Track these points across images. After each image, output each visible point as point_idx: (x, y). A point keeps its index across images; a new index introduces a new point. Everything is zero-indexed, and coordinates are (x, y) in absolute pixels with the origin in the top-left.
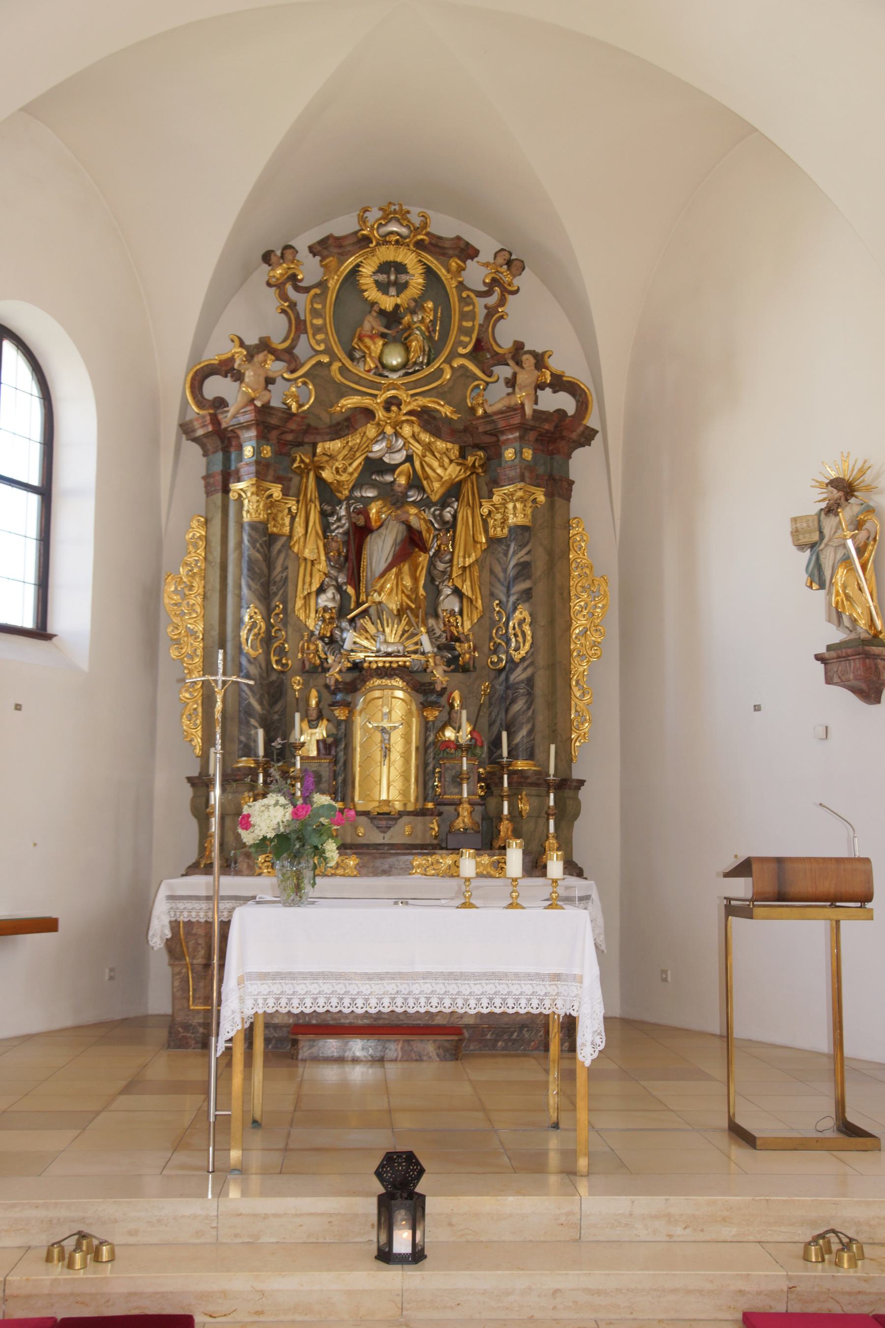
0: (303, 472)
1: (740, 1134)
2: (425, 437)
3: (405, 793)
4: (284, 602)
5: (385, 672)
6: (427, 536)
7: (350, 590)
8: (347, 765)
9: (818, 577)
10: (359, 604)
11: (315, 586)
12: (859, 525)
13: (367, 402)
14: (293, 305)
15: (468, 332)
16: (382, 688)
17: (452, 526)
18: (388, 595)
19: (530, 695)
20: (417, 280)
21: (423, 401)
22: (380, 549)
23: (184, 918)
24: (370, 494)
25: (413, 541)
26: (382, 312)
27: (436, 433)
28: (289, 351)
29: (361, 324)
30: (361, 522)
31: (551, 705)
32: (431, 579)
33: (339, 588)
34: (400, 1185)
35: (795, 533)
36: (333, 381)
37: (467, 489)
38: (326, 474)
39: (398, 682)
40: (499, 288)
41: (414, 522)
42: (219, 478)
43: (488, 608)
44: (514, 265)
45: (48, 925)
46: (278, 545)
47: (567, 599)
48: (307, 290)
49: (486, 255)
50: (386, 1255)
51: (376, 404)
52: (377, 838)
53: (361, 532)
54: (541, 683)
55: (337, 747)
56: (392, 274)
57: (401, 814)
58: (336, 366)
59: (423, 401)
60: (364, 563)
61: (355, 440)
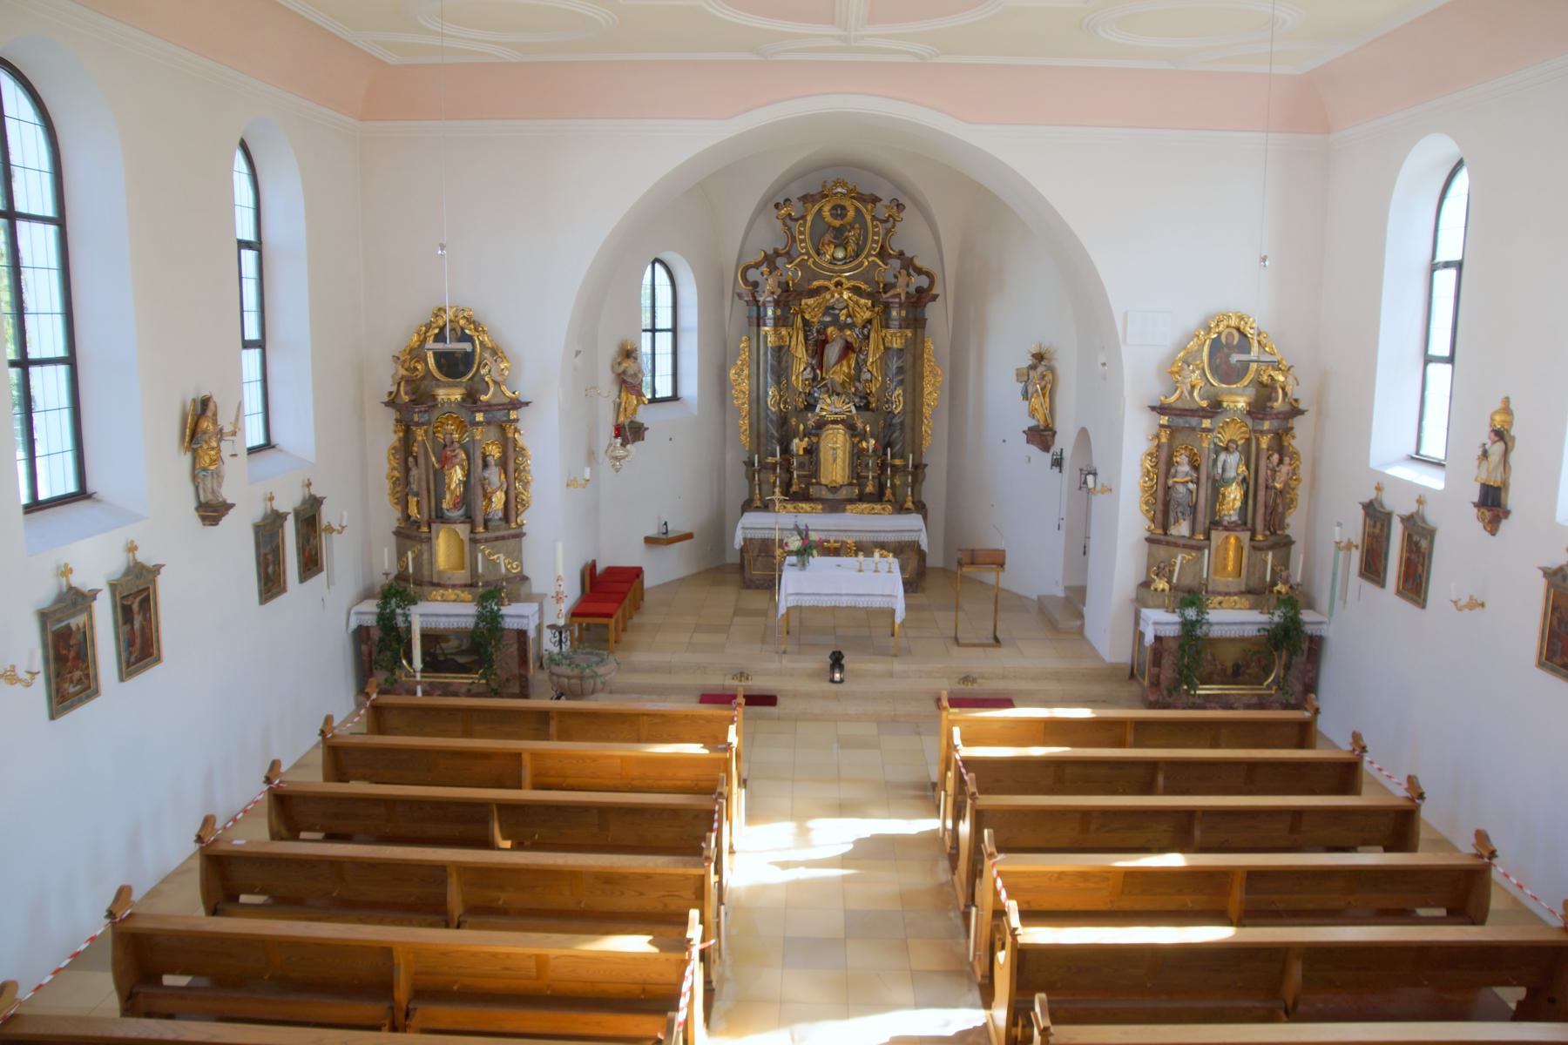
0: (795, 314)
1: (956, 641)
2: (855, 298)
5: (835, 422)
6: (856, 346)
8: (818, 463)
9: (1026, 395)
12: (1043, 377)
15: (877, 242)
17: (868, 337)
18: (838, 373)
19: (902, 430)
20: (851, 213)
22: (832, 352)
24: (828, 319)
25: (848, 348)
27: (861, 296)
28: (788, 253)
29: (822, 235)
31: (913, 429)
33: (813, 369)
34: (837, 661)
43: (884, 381)
45: (689, 536)
49: (886, 201)
50: (832, 681)
52: (830, 496)
53: (825, 342)
54: (908, 421)
55: (811, 451)
56: (839, 211)
61: (819, 299)
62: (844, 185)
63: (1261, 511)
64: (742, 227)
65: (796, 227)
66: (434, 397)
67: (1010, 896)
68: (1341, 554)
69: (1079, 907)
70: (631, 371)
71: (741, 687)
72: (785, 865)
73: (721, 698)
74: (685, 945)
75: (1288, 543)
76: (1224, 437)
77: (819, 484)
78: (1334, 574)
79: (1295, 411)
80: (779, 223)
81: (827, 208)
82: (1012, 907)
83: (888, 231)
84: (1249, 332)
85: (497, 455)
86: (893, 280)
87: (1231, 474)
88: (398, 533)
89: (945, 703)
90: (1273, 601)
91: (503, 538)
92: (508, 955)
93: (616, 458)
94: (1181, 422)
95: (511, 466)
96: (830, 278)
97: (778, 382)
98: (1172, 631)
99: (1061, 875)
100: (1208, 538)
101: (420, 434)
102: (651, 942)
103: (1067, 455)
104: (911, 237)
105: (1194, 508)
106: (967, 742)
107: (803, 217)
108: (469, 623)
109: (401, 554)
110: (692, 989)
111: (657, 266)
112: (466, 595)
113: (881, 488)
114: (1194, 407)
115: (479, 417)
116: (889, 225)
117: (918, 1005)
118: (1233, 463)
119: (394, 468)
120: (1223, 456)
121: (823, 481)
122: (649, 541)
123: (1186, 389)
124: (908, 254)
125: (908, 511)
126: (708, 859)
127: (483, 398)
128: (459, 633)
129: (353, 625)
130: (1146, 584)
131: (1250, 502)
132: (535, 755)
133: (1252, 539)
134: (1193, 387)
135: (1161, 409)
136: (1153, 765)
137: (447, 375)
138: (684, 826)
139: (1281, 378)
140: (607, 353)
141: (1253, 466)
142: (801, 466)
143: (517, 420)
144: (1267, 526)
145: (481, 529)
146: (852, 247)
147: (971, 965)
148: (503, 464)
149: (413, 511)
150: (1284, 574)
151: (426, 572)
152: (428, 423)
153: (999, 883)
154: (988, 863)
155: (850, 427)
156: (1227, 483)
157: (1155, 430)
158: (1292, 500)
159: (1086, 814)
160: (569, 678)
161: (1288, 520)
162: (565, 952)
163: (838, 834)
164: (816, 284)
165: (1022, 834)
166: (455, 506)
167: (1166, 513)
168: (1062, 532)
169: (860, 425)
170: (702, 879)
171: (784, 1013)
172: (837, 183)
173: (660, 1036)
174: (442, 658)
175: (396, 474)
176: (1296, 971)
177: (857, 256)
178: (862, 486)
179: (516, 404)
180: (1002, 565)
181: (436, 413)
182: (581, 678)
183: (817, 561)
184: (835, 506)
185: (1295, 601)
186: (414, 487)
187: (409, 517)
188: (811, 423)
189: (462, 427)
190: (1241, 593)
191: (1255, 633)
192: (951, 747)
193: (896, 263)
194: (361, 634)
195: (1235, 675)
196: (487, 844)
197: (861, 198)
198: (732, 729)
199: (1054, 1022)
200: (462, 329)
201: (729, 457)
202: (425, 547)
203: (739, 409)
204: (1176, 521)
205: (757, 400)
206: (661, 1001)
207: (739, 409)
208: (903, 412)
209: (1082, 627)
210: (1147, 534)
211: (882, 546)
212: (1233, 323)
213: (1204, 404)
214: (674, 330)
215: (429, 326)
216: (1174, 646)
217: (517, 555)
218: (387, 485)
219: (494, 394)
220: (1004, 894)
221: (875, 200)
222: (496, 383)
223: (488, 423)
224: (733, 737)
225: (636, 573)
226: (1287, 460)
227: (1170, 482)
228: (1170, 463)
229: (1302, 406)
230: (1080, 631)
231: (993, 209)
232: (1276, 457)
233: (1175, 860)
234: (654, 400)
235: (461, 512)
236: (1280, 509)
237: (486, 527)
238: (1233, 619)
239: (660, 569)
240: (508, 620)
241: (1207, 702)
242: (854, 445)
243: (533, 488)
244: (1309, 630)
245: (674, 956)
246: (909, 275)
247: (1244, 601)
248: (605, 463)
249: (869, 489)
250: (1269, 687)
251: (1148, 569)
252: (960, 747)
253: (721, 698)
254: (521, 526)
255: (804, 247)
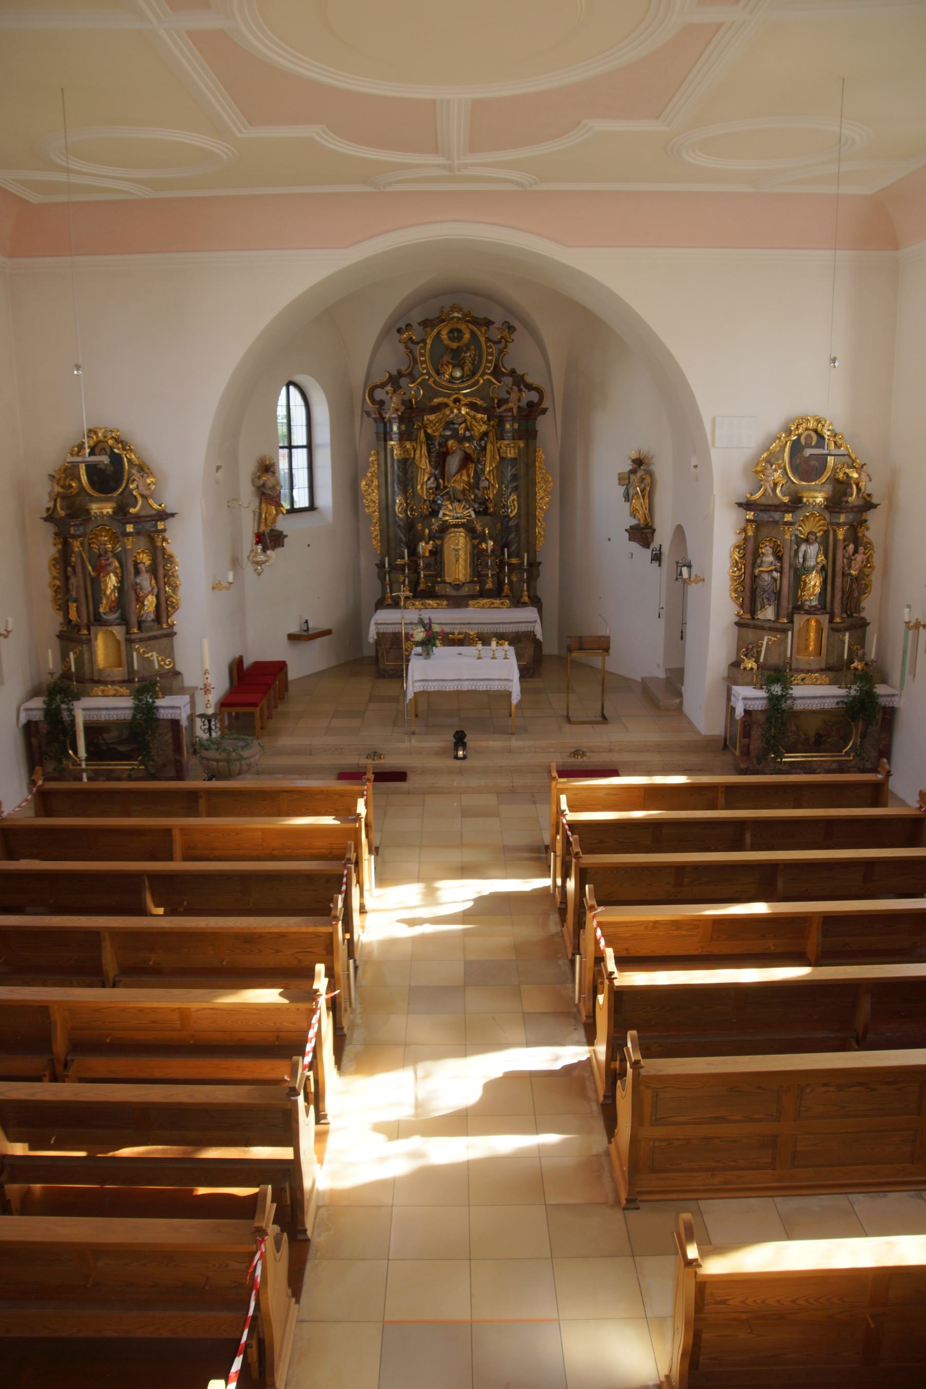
0: (418, 429)
1: (568, 719)
2: (473, 413)
3: (465, 575)
4: (413, 488)
5: (456, 526)
6: (475, 456)
7: (441, 481)
9: (627, 498)
10: (445, 487)
11: (426, 479)
12: (642, 480)
13: (445, 400)
14: (411, 352)
16: (455, 532)
17: (484, 449)
18: (459, 482)
20: (467, 336)
21: (470, 399)
22: (453, 463)
23: (381, 631)
24: (448, 433)
25: (467, 459)
26: (452, 350)
27: (478, 412)
28: (410, 374)
30: (444, 450)
32: (476, 472)
33: (436, 479)
34: (460, 740)
35: (620, 479)
36: (430, 386)
37: (491, 434)
38: (429, 431)
39: (461, 529)
40: (503, 343)
41: (468, 451)
42: (382, 436)
44: (511, 329)
45: (328, 632)
46: (409, 463)
47: (534, 484)
48: (417, 343)
49: (498, 324)
50: (456, 757)
51: (450, 401)
52: (454, 593)
55: (437, 553)
57: (464, 584)
58: (432, 379)
59: (470, 399)
60: (446, 469)
61: (439, 415)
62: (460, 310)
63: (838, 595)
64: (366, 350)
65: (417, 349)
66: (88, 512)
67: (607, 945)
68: (911, 632)
69: (673, 952)
70: (270, 484)
71: (370, 764)
72: (412, 922)
73: (353, 775)
74: (314, 995)
75: (864, 624)
76: (805, 529)
77: (444, 582)
78: (905, 652)
79: (868, 505)
80: (401, 347)
81: (444, 333)
82: (609, 953)
83: (501, 352)
84: (826, 434)
85: (148, 563)
86: (506, 396)
87: (811, 563)
88: (61, 636)
89: (555, 774)
90: (850, 676)
91: (156, 638)
92: (154, 1010)
93: (258, 563)
94: (765, 516)
95: (161, 575)
96: (449, 396)
97: (405, 492)
98: (759, 705)
99: (656, 923)
100: (791, 621)
101: (76, 545)
102: (281, 994)
103: (665, 550)
104: (522, 357)
105: (778, 594)
106: (573, 808)
107: (424, 341)
108: (128, 715)
109: (64, 656)
110: (319, 1034)
111: (292, 388)
112: (124, 690)
113: (500, 584)
114: (777, 502)
115: (130, 528)
116: (502, 346)
117: (528, 1044)
118: (812, 553)
119: (55, 578)
120: (803, 547)
121: (448, 579)
122: (292, 637)
123: (769, 486)
124: (520, 372)
125: (525, 605)
126: (336, 918)
127: (132, 510)
128: (119, 724)
129: (23, 720)
130: (736, 664)
131: (829, 588)
132: (184, 830)
133: (831, 621)
134: (776, 484)
135: (747, 505)
136: (741, 824)
137: (100, 491)
138: (320, 889)
139: (855, 475)
140: (247, 469)
141: (831, 555)
142: (427, 566)
143: (164, 530)
144: (844, 610)
145: (135, 630)
146: (468, 367)
147: (577, 1006)
148: (153, 570)
149: (73, 615)
150: (860, 652)
151: (87, 670)
152: (83, 535)
153: (599, 932)
154: (589, 915)
155: (469, 529)
156: (808, 571)
157: (742, 524)
158: (867, 586)
159: (680, 869)
160: (217, 761)
161: (863, 605)
162: (204, 1005)
163: (460, 893)
164: (436, 401)
165: (617, 889)
166: (112, 610)
167: (753, 601)
168: (662, 623)
169: (479, 528)
170: (331, 936)
171: (407, 1053)
172: (454, 308)
173: (286, 1078)
174: (105, 748)
175: (58, 583)
176: (866, 1005)
177: (473, 374)
178: (482, 583)
179: (164, 516)
180: (607, 650)
181: (91, 526)
182: (228, 761)
183: (440, 650)
184: (458, 602)
185: (871, 675)
186: (74, 593)
187: (71, 621)
188: (435, 527)
189: (115, 538)
190: (821, 670)
191: (834, 706)
192: (561, 813)
193: (509, 380)
194: (29, 729)
195: (817, 743)
196: (142, 911)
197: (476, 321)
198: (361, 802)
199: (644, 1057)
200: (111, 448)
201: (363, 562)
202: (85, 648)
203: (370, 516)
204: (763, 607)
205: (386, 508)
206: (288, 1045)
207: (370, 516)
208: (518, 514)
209: (681, 704)
210: (737, 619)
211: (501, 637)
212: (811, 425)
213: (786, 500)
214: (309, 447)
215: (81, 447)
216: (762, 718)
217: (169, 652)
218: (50, 593)
219: (142, 507)
220: (602, 942)
221: (488, 323)
222: (144, 497)
223: (138, 533)
224: (361, 808)
225: (280, 667)
226: (861, 549)
227: (757, 571)
228: (756, 555)
229: (874, 500)
230: (679, 708)
231: (595, 329)
232: (851, 547)
233: (760, 908)
234: (293, 511)
235: (117, 615)
236: (856, 594)
237: (140, 628)
238: (814, 693)
239: (302, 664)
240: (162, 711)
241: (793, 768)
242: (474, 547)
243: (181, 592)
244: (883, 701)
245: (302, 1006)
246: (520, 390)
247: (825, 678)
248: (248, 568)
249: (489, 585)
250: (847, 754)
251: (738, 650)
252: (567, 812)
253: (353, 775)
254: (171, 626)
255: (424, 368)
